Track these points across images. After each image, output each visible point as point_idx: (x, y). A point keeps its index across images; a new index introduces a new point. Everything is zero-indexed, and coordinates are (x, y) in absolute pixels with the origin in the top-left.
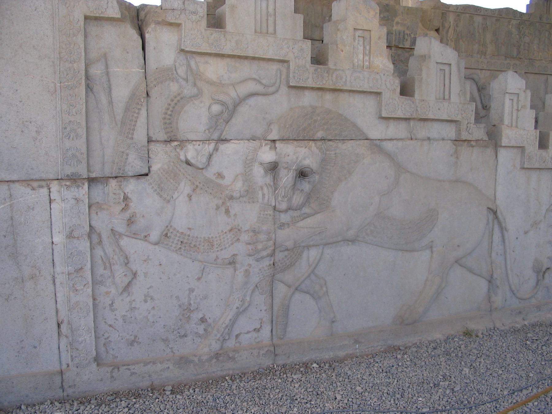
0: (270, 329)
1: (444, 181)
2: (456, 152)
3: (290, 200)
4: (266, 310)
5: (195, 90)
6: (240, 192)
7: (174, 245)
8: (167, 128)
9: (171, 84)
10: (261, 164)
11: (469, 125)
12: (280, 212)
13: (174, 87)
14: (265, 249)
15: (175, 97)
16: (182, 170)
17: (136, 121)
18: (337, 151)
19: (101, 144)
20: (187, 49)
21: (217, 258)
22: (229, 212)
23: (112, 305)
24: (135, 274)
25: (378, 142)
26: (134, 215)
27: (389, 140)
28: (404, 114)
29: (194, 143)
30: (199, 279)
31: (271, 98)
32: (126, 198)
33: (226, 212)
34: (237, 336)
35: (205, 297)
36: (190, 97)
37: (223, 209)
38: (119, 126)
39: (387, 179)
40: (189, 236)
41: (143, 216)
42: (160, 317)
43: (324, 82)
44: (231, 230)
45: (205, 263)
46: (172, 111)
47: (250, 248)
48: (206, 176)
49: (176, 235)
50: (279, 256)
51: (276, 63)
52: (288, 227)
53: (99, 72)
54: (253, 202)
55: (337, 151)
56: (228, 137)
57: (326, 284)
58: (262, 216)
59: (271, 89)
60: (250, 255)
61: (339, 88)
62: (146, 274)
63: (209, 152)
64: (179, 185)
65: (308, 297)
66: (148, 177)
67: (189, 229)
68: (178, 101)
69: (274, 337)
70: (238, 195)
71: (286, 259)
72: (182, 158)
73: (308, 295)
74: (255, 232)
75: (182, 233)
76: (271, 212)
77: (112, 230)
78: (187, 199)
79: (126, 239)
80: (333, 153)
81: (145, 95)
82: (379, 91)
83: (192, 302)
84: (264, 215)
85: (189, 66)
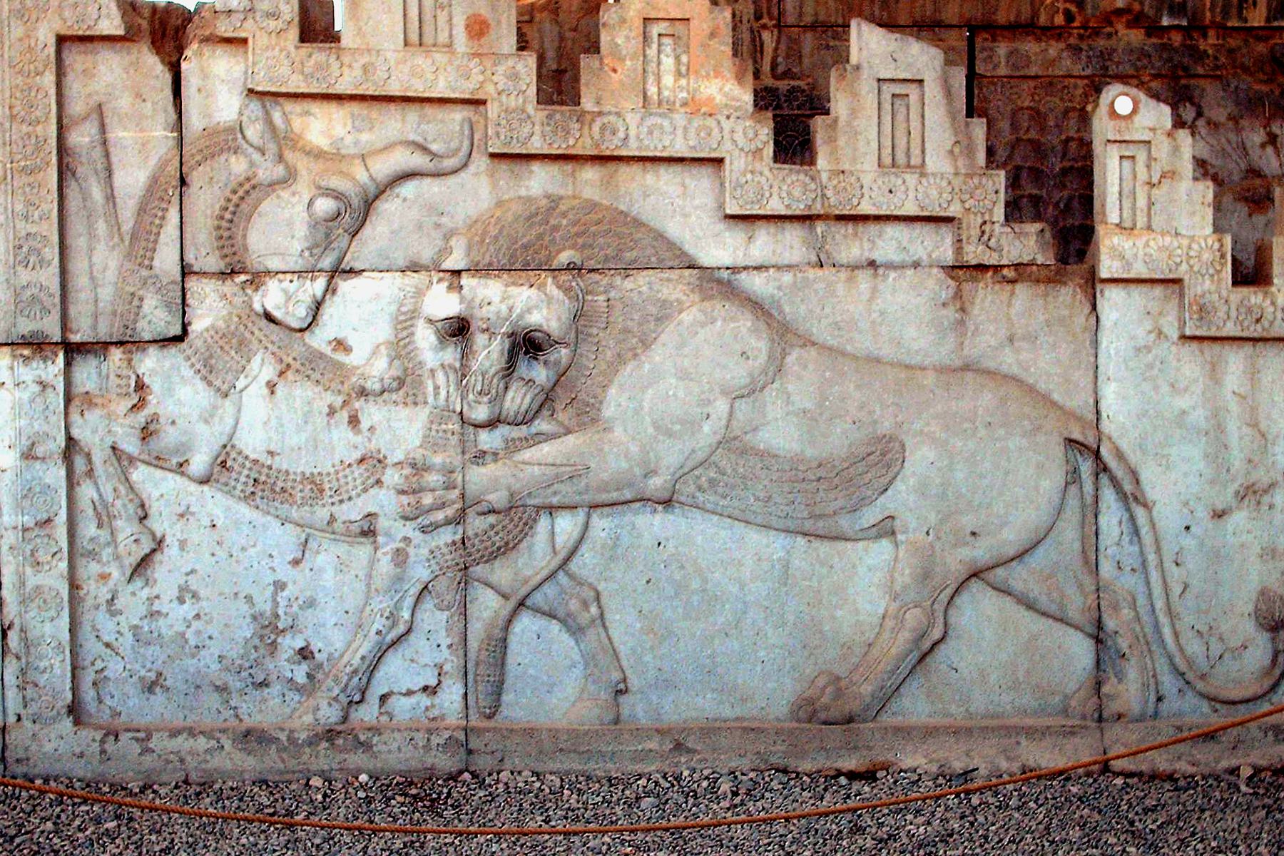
0: (462, 691)
1: (924, 369)
2: (958, 295)
3: (498, 399)
4: (450, 646)
5: (280, 171)
6: (382, 380)
7: (240, 487)
8: (223, 247)
9: (233, 159)
10: (430, 321)
11: (987, 228)
12: (476, 426)
13: (238, 166)
14: (443, 506)
15: (241, 185)
16: (257, 332)
17: (159, 233)
18: (612, 294)
19: (92, 278)
20: (260, 89)
21: (332, 519)
22: (358, 422)
23: (111, 601)
24: (159, 543)
25: (725, 274)
26: (154, 418)
27: (755, 268)
28: (788, 206)
29: (280, 276)
30: (296, 562)
31: (452, 180)
32: (140, 386)
33: (350, 422)
34: (384, 698)
35: (311, 603)
36: (270, 185)
37: (344, 415)
38: (127, 243)
39: (748, 358)
40: (270, 468)
41: (173, 422)
42: (210, 638)
43: (571, 142)
44: (362, 461)
45: (308, 530)
46: (234, 213)
47: (406, 503)
48: (310, 347)
49: (243, 466)
50: (476, 524)
51: (459, 107)
52: (496, 461)
53: (87, 139)
54: (416, 404)
55: (612, 294)
56: (358, 266)
57: (598, 598)
58: (433, 433)
59: (449, 163)
60: (406, 518)
61: (608, 153)
62: (183, 544)
64: (249, 361)
65: (555, 626)
66: (184, 345)
67: (271, 453)
68: (247, 192)
69: (471, 712)
70: (377, 387)
71: (492, 533)
72: (257, 307)
73: (554, 621)
74: (418, 468)
75: (256, 462)
76: (454, 426)
77: (114, 448)
78: (266, 391)
79: (142, 467)
80: (602, 298)
81: (176, 182)
82: (713, 155)
83: (281, 612)
84: (437, 431)
85: (269, 122)
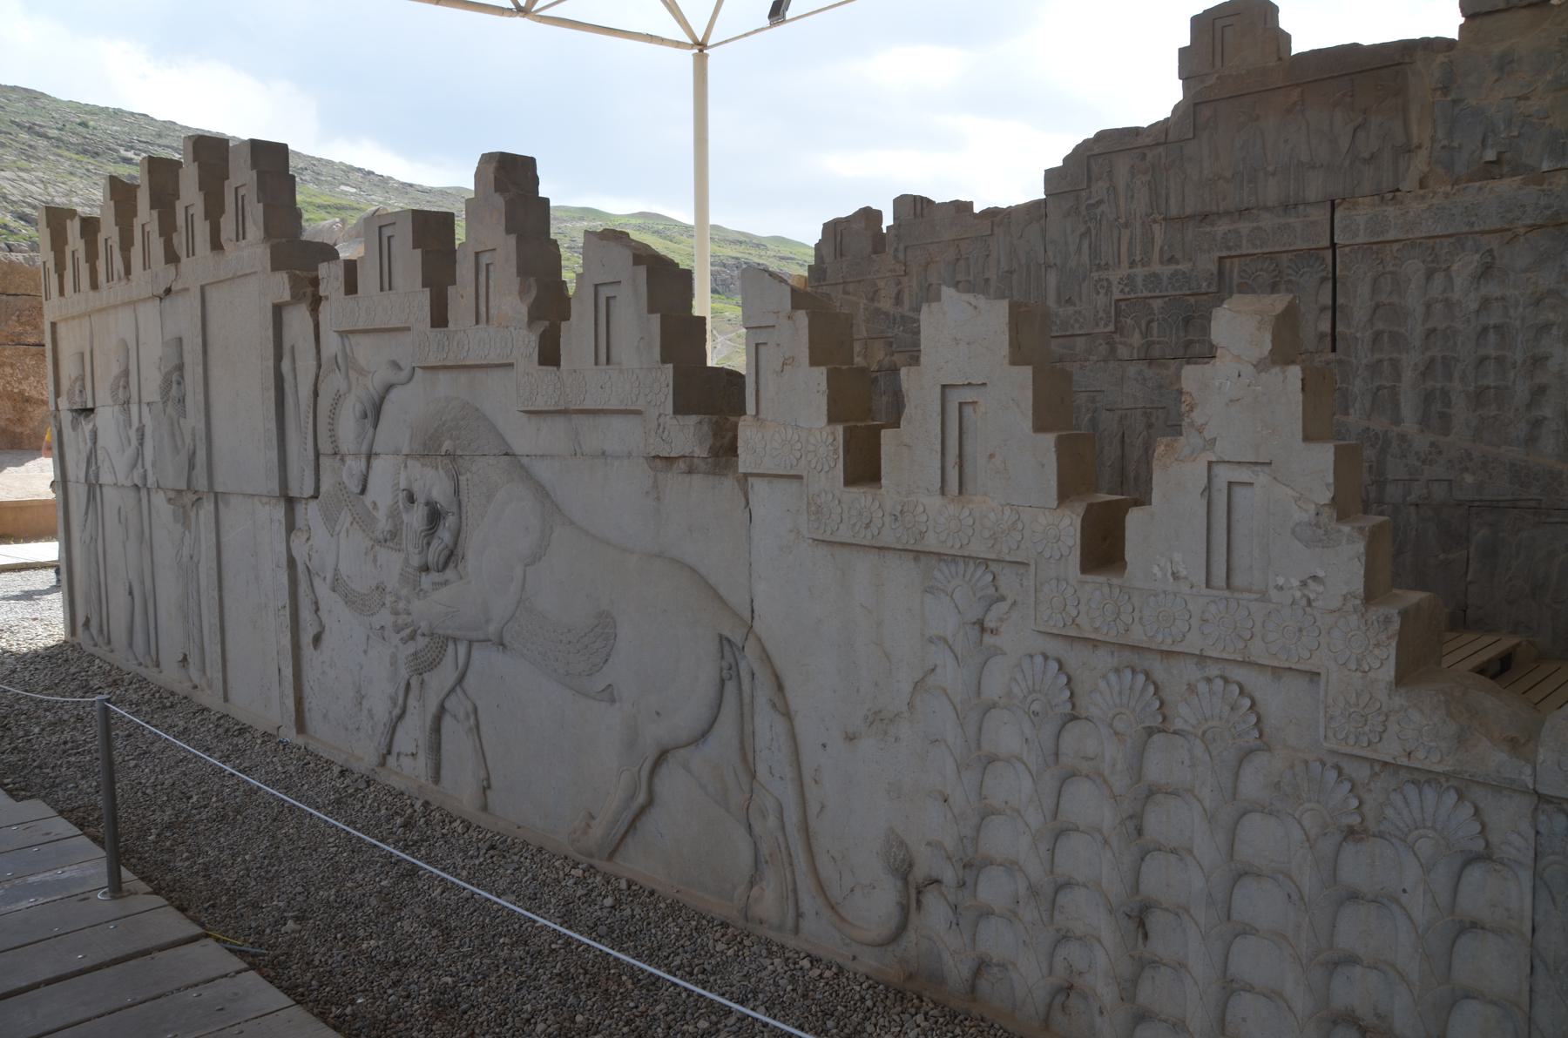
11: (662, 420)
63: (362, 471)
